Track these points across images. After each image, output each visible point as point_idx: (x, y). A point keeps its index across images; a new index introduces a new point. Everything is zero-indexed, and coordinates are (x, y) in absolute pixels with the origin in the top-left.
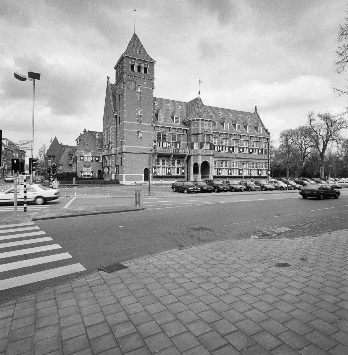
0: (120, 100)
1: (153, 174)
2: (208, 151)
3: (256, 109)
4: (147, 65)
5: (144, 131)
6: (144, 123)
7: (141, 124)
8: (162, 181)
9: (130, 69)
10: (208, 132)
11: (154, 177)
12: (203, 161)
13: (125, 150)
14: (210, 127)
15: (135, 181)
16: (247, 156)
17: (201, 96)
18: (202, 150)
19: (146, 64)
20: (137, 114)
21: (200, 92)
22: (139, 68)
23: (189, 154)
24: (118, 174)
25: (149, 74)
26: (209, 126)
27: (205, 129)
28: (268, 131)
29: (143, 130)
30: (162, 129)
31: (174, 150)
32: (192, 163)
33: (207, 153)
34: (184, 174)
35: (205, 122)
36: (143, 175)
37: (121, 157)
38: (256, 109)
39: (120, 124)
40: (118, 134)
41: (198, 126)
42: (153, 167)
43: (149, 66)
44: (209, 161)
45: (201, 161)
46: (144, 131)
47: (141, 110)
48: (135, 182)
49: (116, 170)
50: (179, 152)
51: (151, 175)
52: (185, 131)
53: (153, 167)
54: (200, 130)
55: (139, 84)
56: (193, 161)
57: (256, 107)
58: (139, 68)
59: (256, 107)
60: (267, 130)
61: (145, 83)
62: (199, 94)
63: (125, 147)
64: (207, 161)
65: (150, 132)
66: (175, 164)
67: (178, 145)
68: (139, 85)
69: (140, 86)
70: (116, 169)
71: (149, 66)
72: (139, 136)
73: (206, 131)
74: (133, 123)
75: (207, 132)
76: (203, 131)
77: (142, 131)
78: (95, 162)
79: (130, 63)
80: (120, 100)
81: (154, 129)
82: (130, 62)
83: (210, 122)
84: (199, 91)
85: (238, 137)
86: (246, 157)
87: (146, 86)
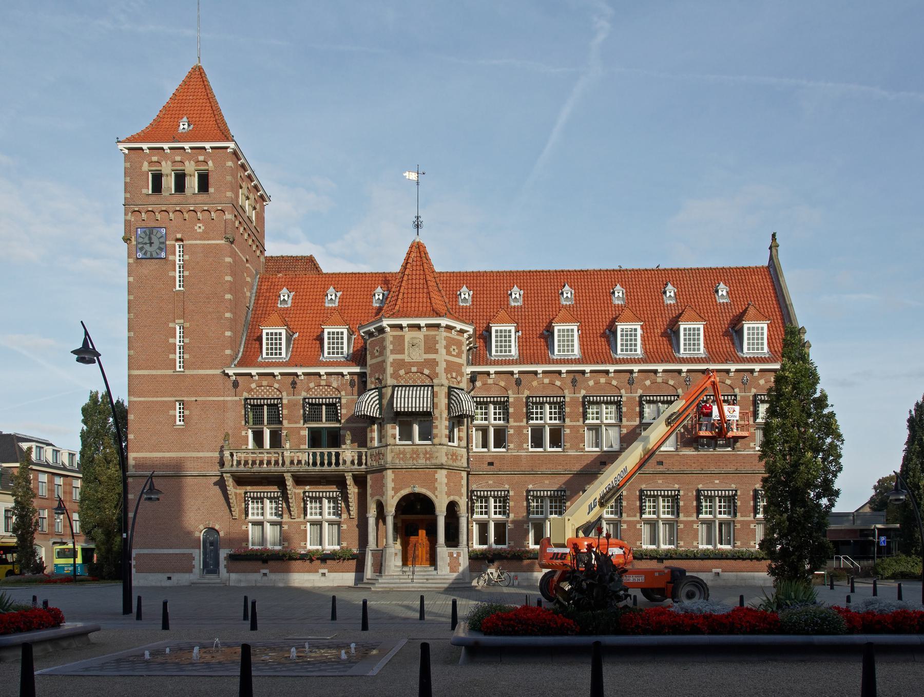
2: (426, 453)
3: (773, 247)
5: (198, 399)
6: (199, 368)
8: (265, 574)
12: (404, 492)
15: (169, 575)
23: (356, 467)
38: (773, 247)
44: (429, 493)
46: (198, 399)
48: (169, 578)
57: (774, 235)
59: (774, 235)
65: (222, 399)
74: (159, 372)
81: (236, 384)
85: (614, 383)
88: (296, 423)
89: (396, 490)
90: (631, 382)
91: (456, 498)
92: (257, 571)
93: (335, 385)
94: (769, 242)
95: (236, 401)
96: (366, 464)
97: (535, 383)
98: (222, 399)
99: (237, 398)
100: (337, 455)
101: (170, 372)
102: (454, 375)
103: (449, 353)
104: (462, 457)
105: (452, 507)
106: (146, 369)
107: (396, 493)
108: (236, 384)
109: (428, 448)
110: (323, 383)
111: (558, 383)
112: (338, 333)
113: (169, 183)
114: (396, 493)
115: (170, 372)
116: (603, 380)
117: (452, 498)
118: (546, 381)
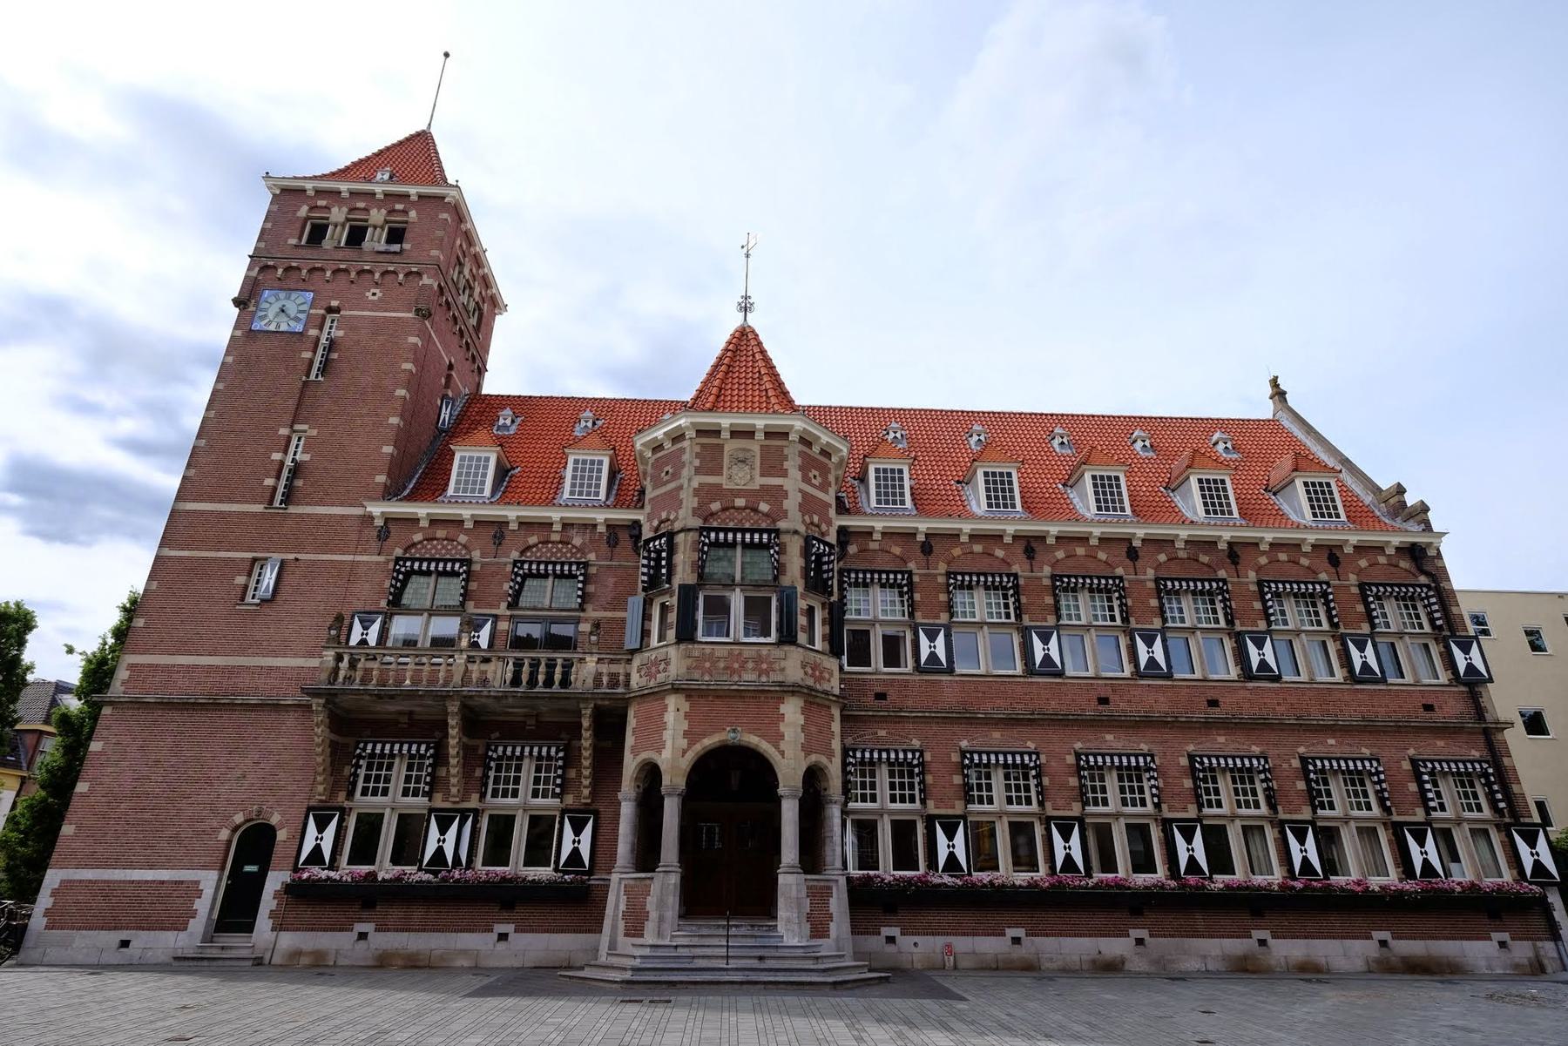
2: (758, 660)
3: (1279, 394)
4: (405, 212)
5: (299, 556)
7: (292, 509)
10: (764, 507)
11: (298, 892)
12: (709, 742)
13: (123, 683)
14: (784, 473)
16: (1226, 701)
17: (754, 321)
18: (696, 650)
19: (399, 207)
28: (1411, 499)
30: (441, 533)
32: (630, 765)
33: (749, 676)
34: (590, 872)
35: (731, 446)
36: (210, 883)
38: (1279, 394)
41: (676, 476)
43: (413, 214)
44: (765, 747)
45: (684, 743)
47: (314, 432)
50: (565, 682)
52: (624, 537)
53: (309, 809)
54: (689, 501)
55: (334, 303)
56: (635, 752)
57: (1274, 382)
59: (1274, 382)
61: (374, 294)
62: (745, 308)
63: (131, 667)
64: (753, 740)
65: (350, 558)
68: (330, 310)
69: (337, 310)
73: (740, 502)
74: (235, 507)
75: (755, 510)
76: (715, 506)
85: (1102, 556)
86: (1215, 713)
87: (375, 306)
88: (491, 606)
89: (691, 736)
91: (824, 760)
93: (577, 541)
94: (1269, 391)
95: (378, 563)
96: (627, 684)
97: (957, 552)
98: (350, 558)
99: (381, 559)
100: (567, 666)
101: (258, 508)
102: (816, 519)
103: (806, 479)
104: (831, 674)
105: (813, 776)
107: (691, 744)
109: (764, 651)
111: (1000, 553)
112: (592, 462)
113: (336, 236)
114: (691, 744)
115: (258, 508)
116: (1080, 551)
117: (814, 758)
118: (978, 548)
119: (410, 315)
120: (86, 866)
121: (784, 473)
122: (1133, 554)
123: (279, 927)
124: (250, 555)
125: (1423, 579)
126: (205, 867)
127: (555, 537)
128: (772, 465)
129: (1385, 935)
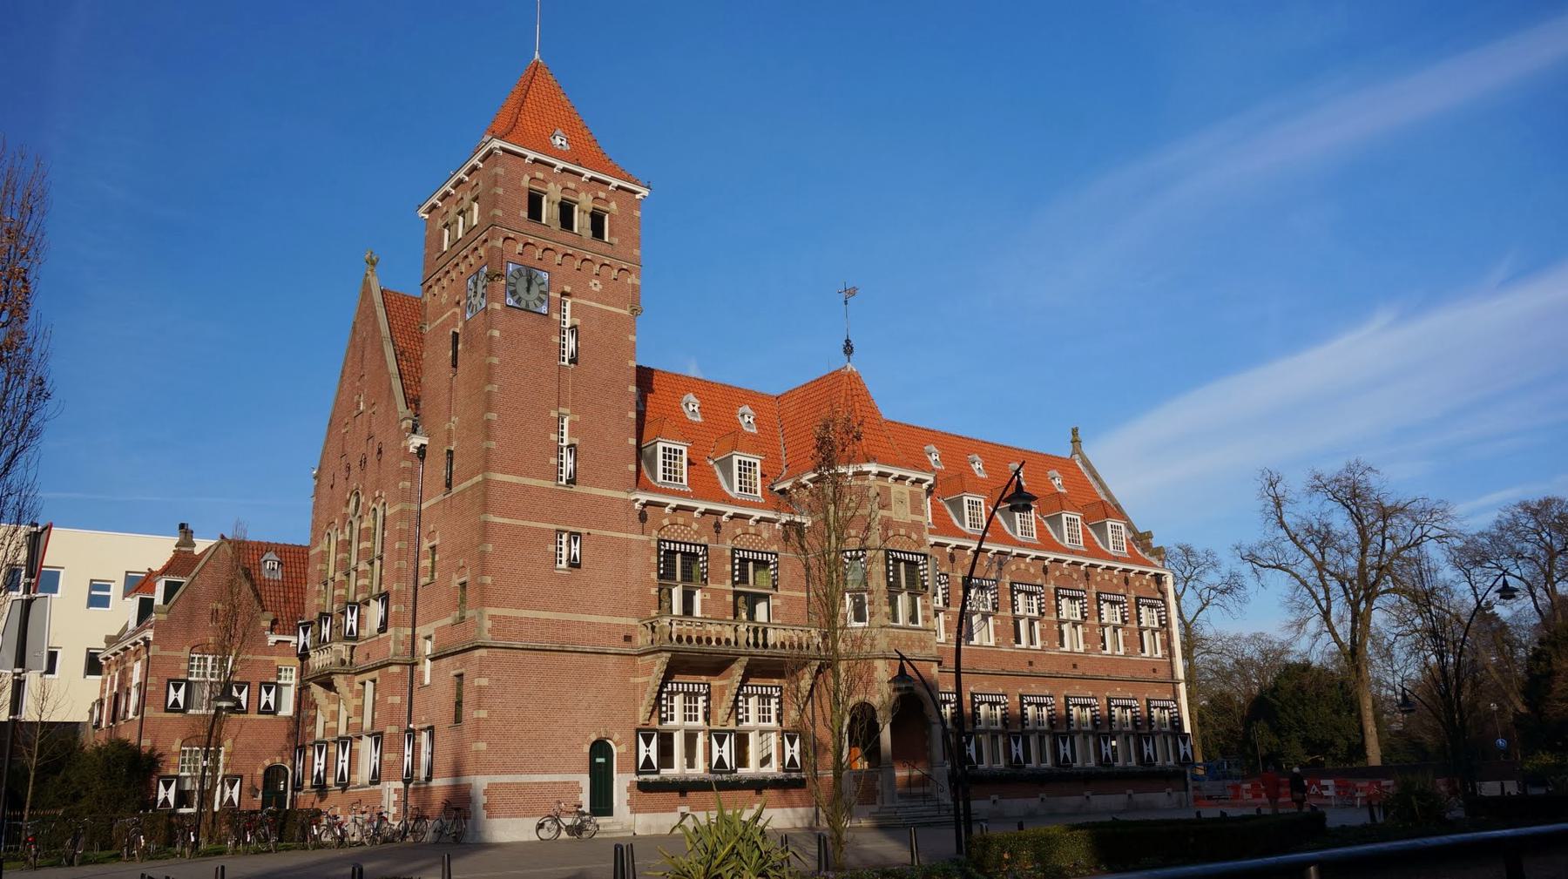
0: (455, 366)
1: (638, 773)
2: (920, 640)
3: (1076, 441)
4: (607, 201)
7: (576, 489)
9: (524, 214)
10: (914, 536)
20: (554, 437)
21: (853, 343)
22: (566, 211)
24: (429, 779)
25: (615, 240)
26: (917, 509)
27: (900, 525)
28: (1155, 543)
29: (587, 524)
31: (751, 635)
35: (896, 488)
36: (585, 781)
37: (460, 676)
38: (1076, 441)
39: (455, 490)
40: (433, 548)
42: (638, 730)
47: (578, 418)
49: (408, 760)
50: (765, 645)
51: (622, 783)
53: (638, 730)
55: (567, 289)
57: (1075, 432)
58: (566, 211)
59: (1075, 432)
60: (1149, 535)
61: (596, 286)
62: (848, 349)
63: (492, 617)
65: (623, 535)
66: (751, 714)
67: (761, 608)
68: (564, 294)
70: (408, 752)
71: (613, 205)
72: (564, 559)
77: (584, 531)
78: (254, 716)
79: (525, 181)
80: (455, 366)
81: (643, 517)
82: (527, 178)
83: (915, 489)
84: (848, 341)
86: (1078, 672)
90: (1045, 570)
92: (673, 810)
98: (623, 535)
99: (645, 538)
101: (550, 484)
106: (514, 473)
108: (643, 517)
110: (752, 530)
115: (550, 484)
119: (626, 313)
120: (503, 773)
121: (922, 513)
122: (1045, 570)
123: (634, 811)
124: (554, 527)
125: (1159, 596)
126: (579, 772)
127: (752, 530)
128: (917, 509)
129: (1130, 791)
